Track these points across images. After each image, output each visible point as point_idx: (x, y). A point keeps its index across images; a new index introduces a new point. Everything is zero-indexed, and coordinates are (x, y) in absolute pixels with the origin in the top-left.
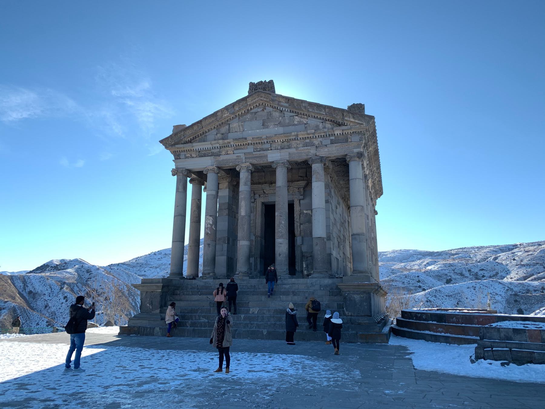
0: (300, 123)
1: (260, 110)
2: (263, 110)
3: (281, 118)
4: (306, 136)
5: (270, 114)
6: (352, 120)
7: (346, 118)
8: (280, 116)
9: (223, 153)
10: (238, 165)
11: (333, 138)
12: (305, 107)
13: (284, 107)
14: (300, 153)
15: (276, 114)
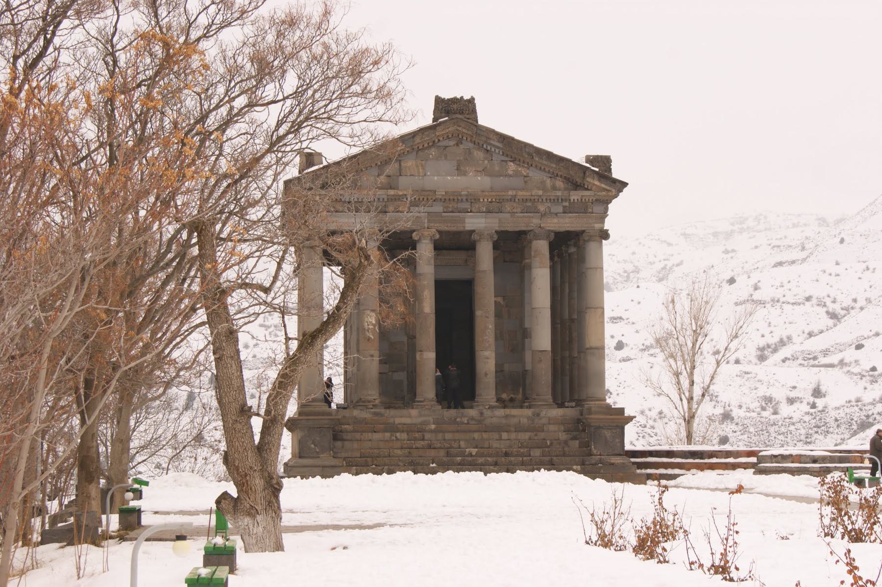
0: (517, 174)
1: (452, 143)
2: (457, 145)
3: (486, 162)
4: (528, 198)
5: (469, 152)
6: (597, 183)
7: (589, 179)
8: (485, 159)
9: (391, 208)
10: (414, 231)
11: (567, 204)
12: (529, 154)
13: (494, 146)
14: (513, 222)
15: (479, 155)
